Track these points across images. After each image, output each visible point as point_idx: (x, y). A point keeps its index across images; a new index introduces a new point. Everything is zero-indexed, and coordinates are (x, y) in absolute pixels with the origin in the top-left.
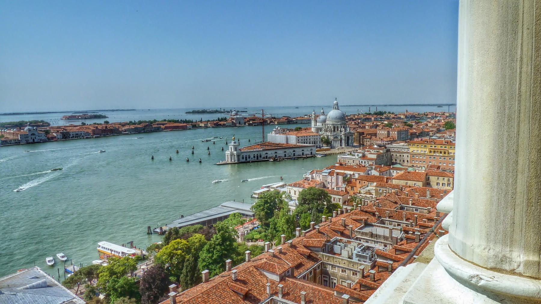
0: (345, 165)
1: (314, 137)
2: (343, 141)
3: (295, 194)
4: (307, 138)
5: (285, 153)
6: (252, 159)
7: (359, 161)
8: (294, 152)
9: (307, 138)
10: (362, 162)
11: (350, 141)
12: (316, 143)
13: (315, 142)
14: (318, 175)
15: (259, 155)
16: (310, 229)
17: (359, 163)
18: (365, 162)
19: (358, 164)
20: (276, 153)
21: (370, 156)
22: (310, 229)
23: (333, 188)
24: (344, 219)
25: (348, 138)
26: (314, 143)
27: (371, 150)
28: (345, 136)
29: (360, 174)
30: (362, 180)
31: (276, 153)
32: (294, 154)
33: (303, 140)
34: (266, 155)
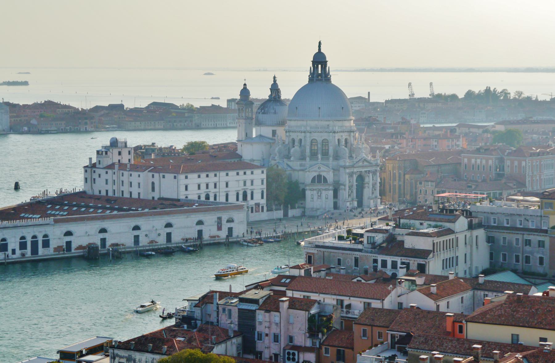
0: (327, 274)
1: (242, 177)
2: (344, 194)
4: (216, 179)
5: (136, 233)
6: (14, 252)
7: (375, 261)
8: (168, 230)
9: (216, 179)
10: (384, 264)
11: (367, 192)
14: (224, 310)
15: (40, 239)
17: (375, 268)
18: (394, 265)
19: (371, 270)
20: (103, 231)
21: (410, 242)
23: (276, 355)
25: (361, 178)
27: (417, 223)
28: (351, 175)
29: (369, 304)
30: (372, 326)
31: (103, 231)
32: (169, 235)
33: (203, 187)
34: (68, 239)
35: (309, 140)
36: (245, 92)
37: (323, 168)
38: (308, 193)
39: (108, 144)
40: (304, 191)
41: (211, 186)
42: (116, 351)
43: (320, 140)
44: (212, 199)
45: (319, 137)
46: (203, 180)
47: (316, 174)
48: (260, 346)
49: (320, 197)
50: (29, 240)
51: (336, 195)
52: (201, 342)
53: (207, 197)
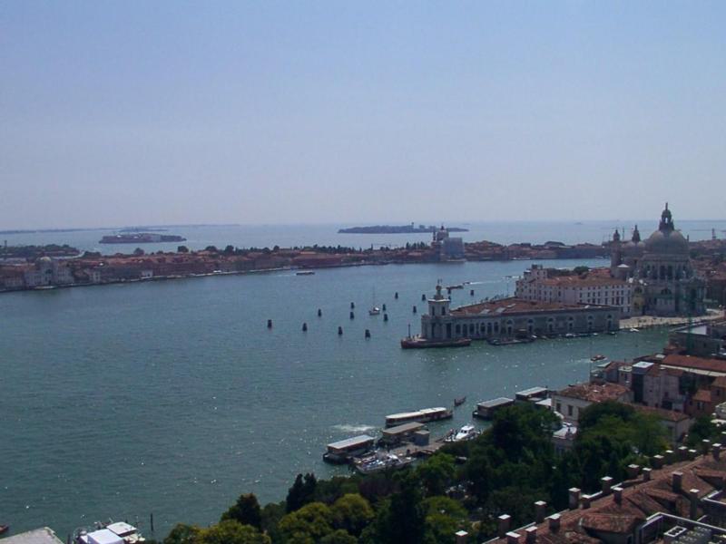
1: (616, 289)
2: (682, 303)
3: (570, 414)
12: (620, 302)
13: (618, 298)
16: (601, 492)
22: (601, 492)
24: (680, 474)
25: (694, 293)
26: (615, 302)
28: (687, 288)
33: (591, 295)
35: (659, 266)
36: (617, 235)
37: (669, 284)
38: (658, 300)
39: (530, 267)
40: (656, 300)
41: (596, 295)
42: (557, 398)
43: (666, 266)
44: (596, 303)
45: (666, 264)
46: (591, 291)
47: (663, 288)
48: (645, 400)
49: (666, 303)
50: (486, 324)
51: (677, 302)
52: (610, 394)
53: (594, 301)
